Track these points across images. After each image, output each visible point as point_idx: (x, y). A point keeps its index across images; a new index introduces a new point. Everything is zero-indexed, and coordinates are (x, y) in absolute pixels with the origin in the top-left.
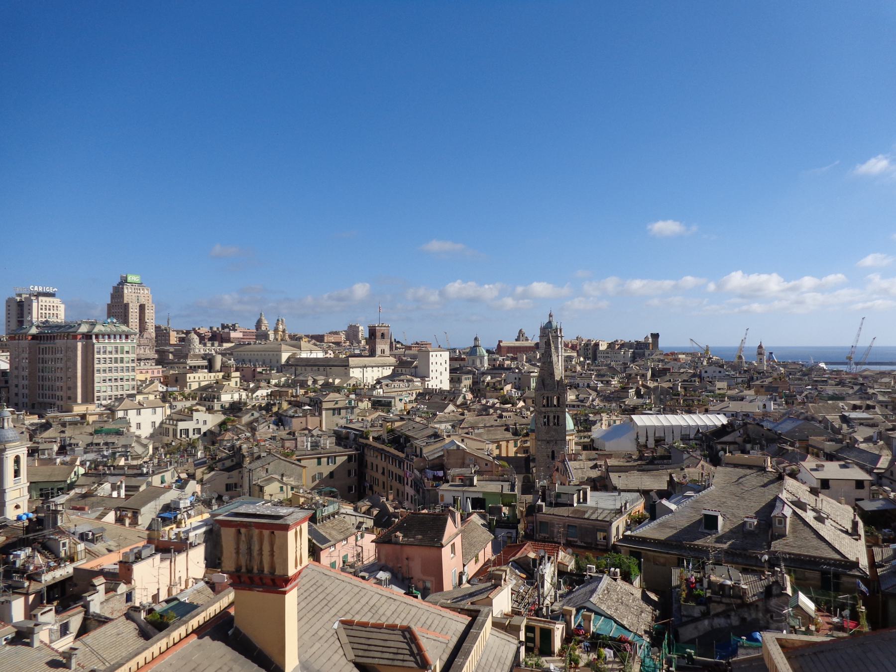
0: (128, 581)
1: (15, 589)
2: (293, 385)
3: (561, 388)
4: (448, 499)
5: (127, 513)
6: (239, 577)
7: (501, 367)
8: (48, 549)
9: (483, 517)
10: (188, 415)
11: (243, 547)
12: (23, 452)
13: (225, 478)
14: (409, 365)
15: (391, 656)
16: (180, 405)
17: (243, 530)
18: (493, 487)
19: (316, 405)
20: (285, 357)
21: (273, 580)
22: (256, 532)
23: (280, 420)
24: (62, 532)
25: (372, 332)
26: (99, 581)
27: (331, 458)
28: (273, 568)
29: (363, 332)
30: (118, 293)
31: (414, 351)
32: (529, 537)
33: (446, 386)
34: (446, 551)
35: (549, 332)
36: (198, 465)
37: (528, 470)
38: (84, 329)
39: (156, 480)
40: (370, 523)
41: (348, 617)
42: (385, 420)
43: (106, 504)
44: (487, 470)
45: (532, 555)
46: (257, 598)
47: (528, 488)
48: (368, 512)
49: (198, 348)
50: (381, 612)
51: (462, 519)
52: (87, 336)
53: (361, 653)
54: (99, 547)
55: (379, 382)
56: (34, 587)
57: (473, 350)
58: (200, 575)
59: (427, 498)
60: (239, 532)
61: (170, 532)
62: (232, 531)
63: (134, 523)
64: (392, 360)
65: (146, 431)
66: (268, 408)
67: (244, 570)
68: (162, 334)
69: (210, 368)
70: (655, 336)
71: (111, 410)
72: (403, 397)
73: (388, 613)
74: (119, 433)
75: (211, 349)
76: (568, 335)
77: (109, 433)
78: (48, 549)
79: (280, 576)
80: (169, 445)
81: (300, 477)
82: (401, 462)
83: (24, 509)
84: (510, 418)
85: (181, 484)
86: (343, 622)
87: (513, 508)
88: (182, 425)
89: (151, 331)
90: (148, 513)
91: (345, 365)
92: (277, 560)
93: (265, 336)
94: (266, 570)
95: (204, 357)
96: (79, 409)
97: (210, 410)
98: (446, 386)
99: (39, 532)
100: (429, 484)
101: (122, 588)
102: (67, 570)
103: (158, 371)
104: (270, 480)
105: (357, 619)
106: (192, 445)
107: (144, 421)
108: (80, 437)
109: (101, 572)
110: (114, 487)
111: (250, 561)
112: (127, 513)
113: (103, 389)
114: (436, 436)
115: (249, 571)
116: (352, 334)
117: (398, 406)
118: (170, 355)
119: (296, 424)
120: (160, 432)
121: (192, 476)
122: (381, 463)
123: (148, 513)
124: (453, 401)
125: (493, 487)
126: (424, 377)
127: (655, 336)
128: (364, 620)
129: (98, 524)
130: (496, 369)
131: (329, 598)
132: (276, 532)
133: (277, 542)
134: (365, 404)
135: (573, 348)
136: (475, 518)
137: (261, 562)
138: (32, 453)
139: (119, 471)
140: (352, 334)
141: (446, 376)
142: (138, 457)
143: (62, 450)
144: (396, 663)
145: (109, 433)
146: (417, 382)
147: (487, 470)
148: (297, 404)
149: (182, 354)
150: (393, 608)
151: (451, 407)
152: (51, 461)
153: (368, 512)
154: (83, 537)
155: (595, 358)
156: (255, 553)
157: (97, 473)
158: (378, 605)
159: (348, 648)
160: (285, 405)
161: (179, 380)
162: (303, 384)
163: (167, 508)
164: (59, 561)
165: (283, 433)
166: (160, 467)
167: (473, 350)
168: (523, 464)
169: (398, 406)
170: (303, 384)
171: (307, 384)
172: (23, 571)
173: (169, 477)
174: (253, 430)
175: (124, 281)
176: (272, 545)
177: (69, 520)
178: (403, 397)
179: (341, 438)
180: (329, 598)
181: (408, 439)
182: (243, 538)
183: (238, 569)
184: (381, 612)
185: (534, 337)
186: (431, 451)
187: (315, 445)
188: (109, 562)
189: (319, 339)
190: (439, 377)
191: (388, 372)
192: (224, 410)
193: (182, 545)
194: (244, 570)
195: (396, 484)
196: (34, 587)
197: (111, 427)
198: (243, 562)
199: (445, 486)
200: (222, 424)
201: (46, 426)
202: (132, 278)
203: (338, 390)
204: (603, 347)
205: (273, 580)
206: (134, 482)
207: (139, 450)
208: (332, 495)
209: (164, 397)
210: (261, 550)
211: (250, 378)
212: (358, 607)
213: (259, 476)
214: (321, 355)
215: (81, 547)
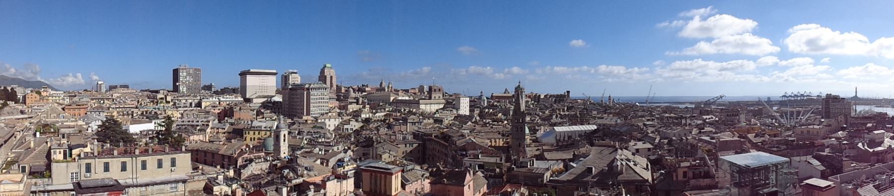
0: (325, 189)
1: (284, 184)
2: (395, 111)
3: (523, 115)
4: (468, 164)
5: (325, 161)
7: (493, 105)
8: (294, 171)
9: (483, 173)
10: (348, 122)
12: (286, 133)
13: (362, 150)
14: (451, 103)
16: (346, 118)
18: (492, 160)
19: (405, 121)
20: (392, 99)
23: (390, 127)
24: (299, 165)
25: (430, 88)
26: (312, 187)
27: (411, 144)
29: (426, 89)
30: (323, 71)
31: (453, 97)
32: (508, 182)
33: (468, 113)
34: (466, 188)
35: (519, 90)
36: (352, 144)
37: (508, 152)
38: (307, 86)
39: (335, 148)
40: (428, 175)
42: (440, 128)
43: (317, 156)
44: (486, 152)
45: (509, 190)
47: (508, 160)
48: (427, 170)
49: (353, 94)
51: (474, 174)
52: (308, 89)
54: (311, 173)
55: (437, 111)
56: (290, 185)
57: (480, 98)
58: (352, 190)
59: (459, 164)
61: (340, 171)
63: (327, 165)
64: (444, 101)
65: (332, 128)
66: (384, 121)
68: (339, 88)
69: (357, 103)
70: (568, 92)
71: (316, 119)
72: (448, 118)
74: (322, 128)
75: (358, 95)
76: (527, 91)
77: (318, 128)
78: (294, 171)
80: (341, 135)
81: (397, 152)
82: (446, 147)
83: (286, 155)
84: (501, 128)
85: (345, 151)
87: (501, 169)
88: (346, 127)
89: (335, 87)
90: (332, 162)
91: (418, 103)
93: (384, 90)
95: (355, 98)
96: (305, 118)
97: (357, 121)
98: (468, 113)
99: (291, 164)
100: (459, 157)
101: (322, 191)
102: (300, 180)
103: (337, 103)
104: (385, 153)
106: (350, 135)
107: (332, 124)
108: (306, 129)
109: (314, 184)
110: (320, 150)
112: (325, 161)
113: (315, 110)
114: (463, 136)
116: (421, 89)
117: (446, 122)
118: (342, 97)
119: (396, 128)
120: (337, 129)
121: (349, 148)
122: (437, 147)
123: (332, 162)
124: (471, 120)
125: (492, 160)
126: (458, 109)
127: (568, 92)
129: (313, 164)
130: (491, 106)
134: (431, 121)
135: (529, 97)
136: (479, 173)
138: (289, 133)
139: (321, 144)
140: (421, 89)
141: (468, 108)
142: (329, 138)
143: (299, 134)
145: (318, 128)
146: (455, 112)
147: (486, 152)
148: (397, 120)
149: (346, 96)
151: (470, 123)
152: (295, 137)
153: (427, 170)
154: (306, 168)
155: (538, 102)
157: (313, 143)
160: (392, 120)
161: (345, 108)
162: (400, 111)
163: (339, 160)
164: (298, 176)
165: (391, 132)
166: (337, 143)
167: (480, 98)
168: (505, 150)
169: (446, 122)
170: (400, 111)
171: (403, 111)
172: (286, 177)
173: (341, 147)
174: (378, 130)
175: (325, 67)
177: (303, 162)
178: (448, 118)
179: (416, 135)
181: (450, 137)
185: (512, 92)
186: (460, 143)
187: (404, 138)
188: (318, 180)
189: (407, 91)
190: (464, 109)
191: (442, 106)
192: (363, 121)
193: (345, 177)
195: (444, 157)
196: (290, 185)
197: (318, 127)
199: (466, 159)
200: (362, 127)
201: (294, 124)
202: (328, 65)
203: (415, 114)
204: (542, 97)
206: (327, 148)
207: (329, 135)
208: (411, 161)
209: (339, 114)
211: (374, 108)
213: (380, 151)
214: (407, 98)
215: (305, 172)
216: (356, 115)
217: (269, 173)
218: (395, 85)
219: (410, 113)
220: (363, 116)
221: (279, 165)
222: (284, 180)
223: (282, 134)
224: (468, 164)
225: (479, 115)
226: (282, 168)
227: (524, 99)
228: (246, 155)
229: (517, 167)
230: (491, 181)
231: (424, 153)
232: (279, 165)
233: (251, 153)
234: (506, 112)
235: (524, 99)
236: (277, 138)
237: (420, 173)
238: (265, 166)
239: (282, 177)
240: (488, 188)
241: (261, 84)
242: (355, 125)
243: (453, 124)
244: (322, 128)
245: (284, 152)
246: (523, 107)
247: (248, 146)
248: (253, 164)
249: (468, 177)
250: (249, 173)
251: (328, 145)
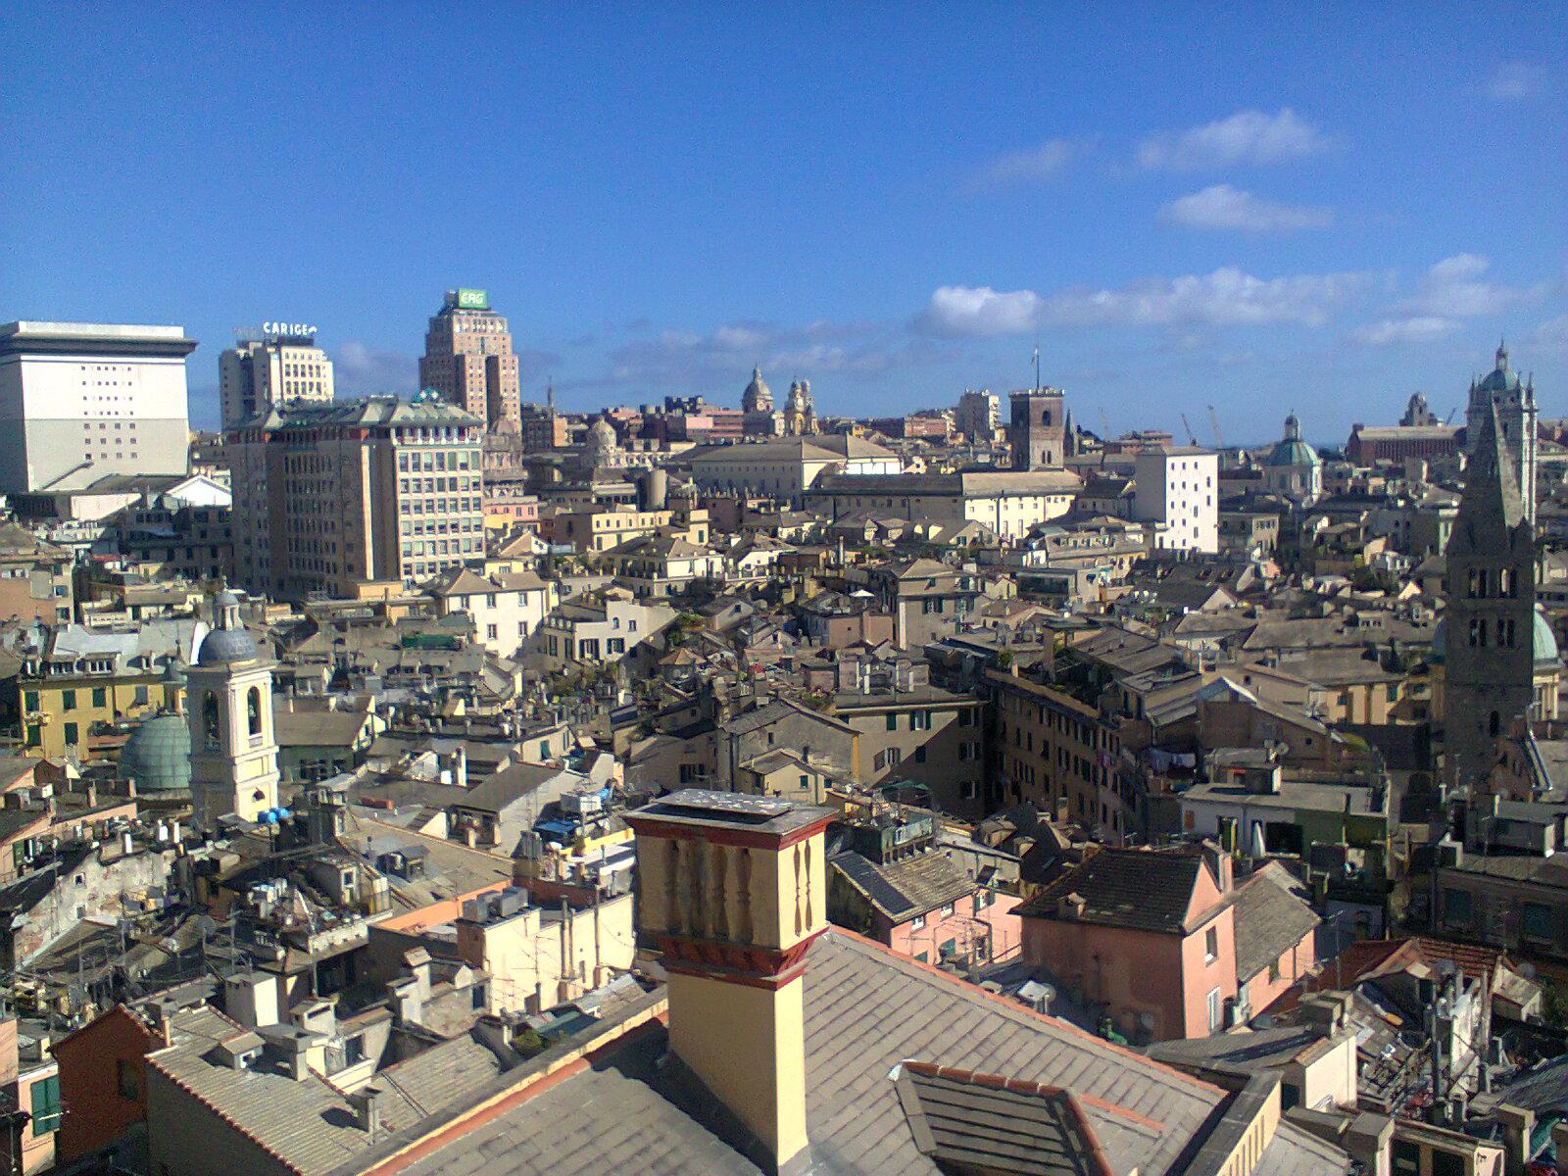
1: (261, 963)
2: (830, 539)
3: (1522, 547)
4: (1206, 821)
5: (472, 819)
6: (676, 944)
7: (1359, 494)
8: (318, 884)
9: (1294, 869)
10: (595, 608)
11: (683, 880)
12: (263, 681)
13: (676, 752)
14: (1118, 490)
15: (1020, 1153)
16: (582, 585)
17: (682, 844)
18: (1325, 799)
19: (885, 589)
20: (810, 472)
21: (748, 956)
22: (709, 848)
23: (802, 623)
24: (344, 852)
25: (1020, 409)
27: (920, 716)
28: (747, 928)
29: (997, 408)
30: (440, 332)
31: (1127, 456)
33: (1209, 542)
35: (1495, 402)
36: (618, 722)
37: (1424, 760)
38: (373, 415)
39: (530, 751)
40: (1011, 872)
41: (925, 1059)
42: (1049, 625)
43: (429, 799)
44: (1310, 754)
46: (714, 992)
47: (1419, 804)
48: (1007, 845)
49: (615, 455)
50: (1003, 1054)
52: (380, 432)
53: (950, 1139)
54: (416, 887)
55: (1036, 532)
56: (295, 961)
57: (1282, 453)
58: (626, 964)
61: (563, 864)
63: (487, 841)
64: (1070, 478)
65: (507, 644)
66: (772, 593)
67: (685, 930)
68: (536, 424)
69: (643, 501)
71: (436, 595)
72: (1098, 573)
73: (1021, 1060)
74: (452, 646)
75: (645, 456)
77: (431, 645)
78: (318, 884)
79: (763, 948)
80: (558, 674)
81: (845, 755)
82: (1088, 729)
83: (270, 802)
84: (1377, 625)
85: (583, 761)
86: (909, 1067)
87: (1375, 853)
88: (584, 631)
89: (513, 416)
90: (514, 821)
91: (954, 494)
92: (757, 913)
93: (768, 426)
94: (733, 931)
95: (628, 476)
96: (370, 593)
97: (643, 597)
98: (1209, 542)
99: (300, 847)
100: (1158, 784)
102: (353, 933)
103: (530, 508)
104: (777, 762)
106: (606, 675)
107: (504, 621)
108: (376, 657)
109: (423, 941)
110: (444, 762)
111: (699, 911)
112: (472, 819)
113: (417, 549)
114: (1179, 666)
115: (697, 933)
116: (971, 415)
117: (1086, 593)
118: (554, 472)
119: (838, 632)
120: (537, 645)
121: (605, 745)
122: (1042, 731)
123: (514, 821)
124: (1227, 581)
125: (1325, 799)
126: (1152, 518)
128: (962, 1067)
129: (410, 839)
130: (1343, 499)
131: (882, 1013)
132: (752, 851)
133: (756, 873)
134: (1002, 588)
136: (1274, 871)
138: (280, 684)
139: (453, 728)
140: (971, 415)
141: (1210, 516)
142: (491, 700)
143: (340, 682)
145: (431, 645)
146: (1134, 534)
147: (1310, 754)
148: (843, 587)
149: (581, 466)
150: (1033, 1048)
151: (1220, 597)
152: (319, 702)
153: (1007, 845)
154: (385, 865)
156: (709, 895)
157: (412, 729)
158: (997, 1039)
159: (922, 1126)
160: (812, 589)
161: (575, 529)
162: (854, 539)
163: (552, 811)
164: (342, 912)
165: (807, 654)
166: (538, 724)
167: (1282, 453)
168: (1409, 746)
169: (1086, 593)
170: (854, 539)
172: (272, 926)
173: (557, 744)
174: (740, 645)
175: (452, 306)
177: (355, 827)
178: (1098, 573)
179: (943, 667)
180: (882, 1013)
181: (1107, 673)
182: (682, 861)
183: (674, 929)
184: (1003, 1054)
185: (1450, 416)
186: (1165, 706)
187: (881, 683)
188: (438, 920)
189: (891, 429)
190: (1191, 515)
191: (1060, 508)
192: (675, 598)
193: (584, 895)
194: (685, 930)
195: (1076, 782)
196: (295, 961)
197: (434, 632)
199: (1198, 792)
200: (671, 631)
201: (306, 629)
202: (470, 297)
203: (936, 551)
205: (748, 956)
206: (485, 753)
207: (495, 684)
208: (924, 802)
209: (546, 568)
210: (721, 889)
211: (733, 524)
212: (948, 1039)
213: (753, 751)
214: (894, 467)
215: (381, 884)
216: (637, 566)
217: (168, 913)
218: (819, 401)
219: (913, 546)
220: (678, 570)
221: (229, 861)
222: (261, 940)
223: (238, 689)
224: (1206, 821)
225: (1276, 554)
226: (243, 880)
227: (1533, 456)
228: (41, 828)
229: (1474, 849)
230: (1339, 911)
231: (992, 760)
232: (229, 861)
233: (79, 808)
234: (1410, 538)
235: (1533, 456)
236: (211, 712)
237: (967, 864)
238: (146, 877)
239: (249, 922)
240: (1320, 951)
241: (95, 410)
242: (634, 621)
243: (1129, 605)
244: (452, 646)
245: (257, 783)
246: (1521, 502)
247: (47, 772)
248: (91, 869)
249: (1205, 890)
250: (67, 923)
251: (489, 732)
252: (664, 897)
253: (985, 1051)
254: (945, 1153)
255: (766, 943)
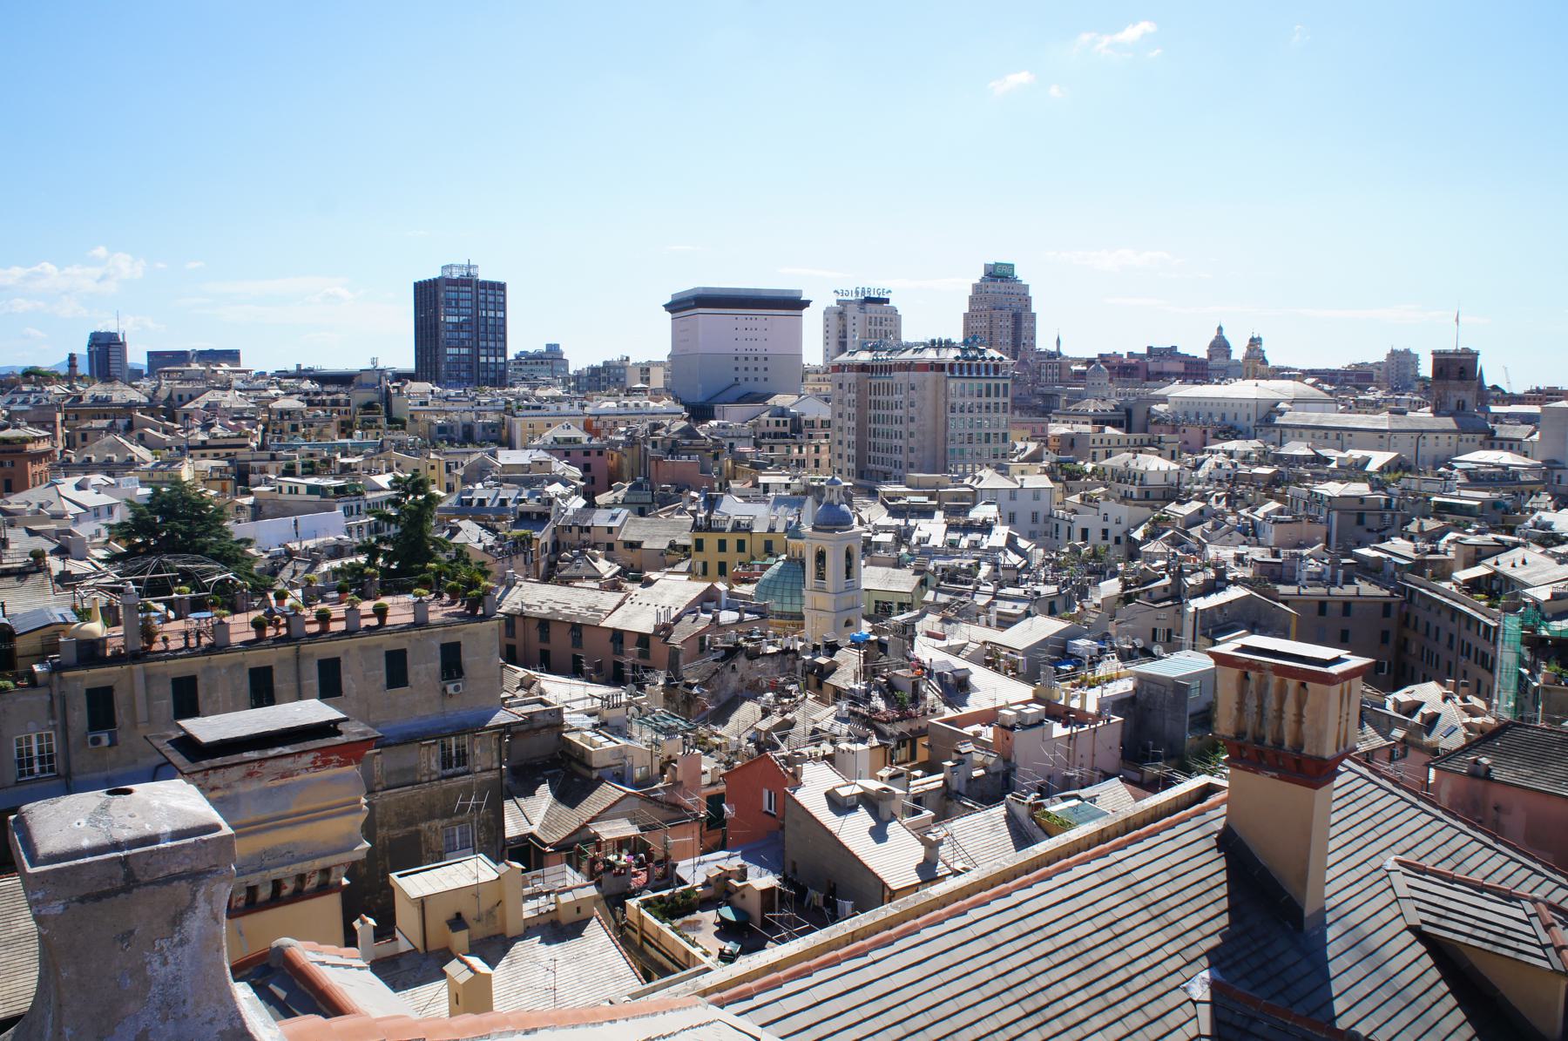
11: (1252, 703)
15: (1491, 937)
17: (1252, 674)
22: (1274, 680)
28: (1298, 745)
53: (1433, 919)
60: (1246, 676)
62: (1235, 673)
67: (1249, 737)
79: (1310, 758)
86: (1402, 863)
94: (1288, 742)
105: (1428, 863)
115: (1259, 740)
132: (1309, 685)
133: (1311, 700)
137: (1280, 728)
144: (1500, 950)
176: (1300, 704)
182: (1252, 685)
183: (1240, 734)
184: (1471, 864)
194: (1249, 737)
198: (1250, 723)
205: (1298, 762)
210: (1280, 711)
252: (1235, 712)
253: (1458, 858)
254: (1426, 928)
255: (1313, 752)
